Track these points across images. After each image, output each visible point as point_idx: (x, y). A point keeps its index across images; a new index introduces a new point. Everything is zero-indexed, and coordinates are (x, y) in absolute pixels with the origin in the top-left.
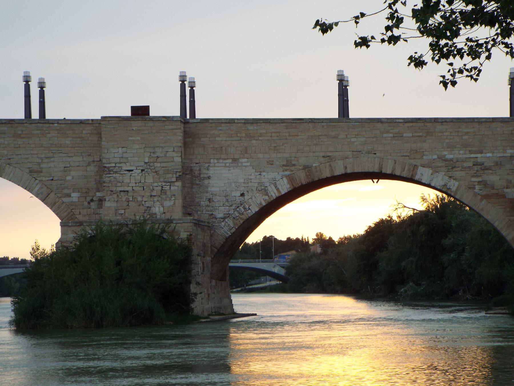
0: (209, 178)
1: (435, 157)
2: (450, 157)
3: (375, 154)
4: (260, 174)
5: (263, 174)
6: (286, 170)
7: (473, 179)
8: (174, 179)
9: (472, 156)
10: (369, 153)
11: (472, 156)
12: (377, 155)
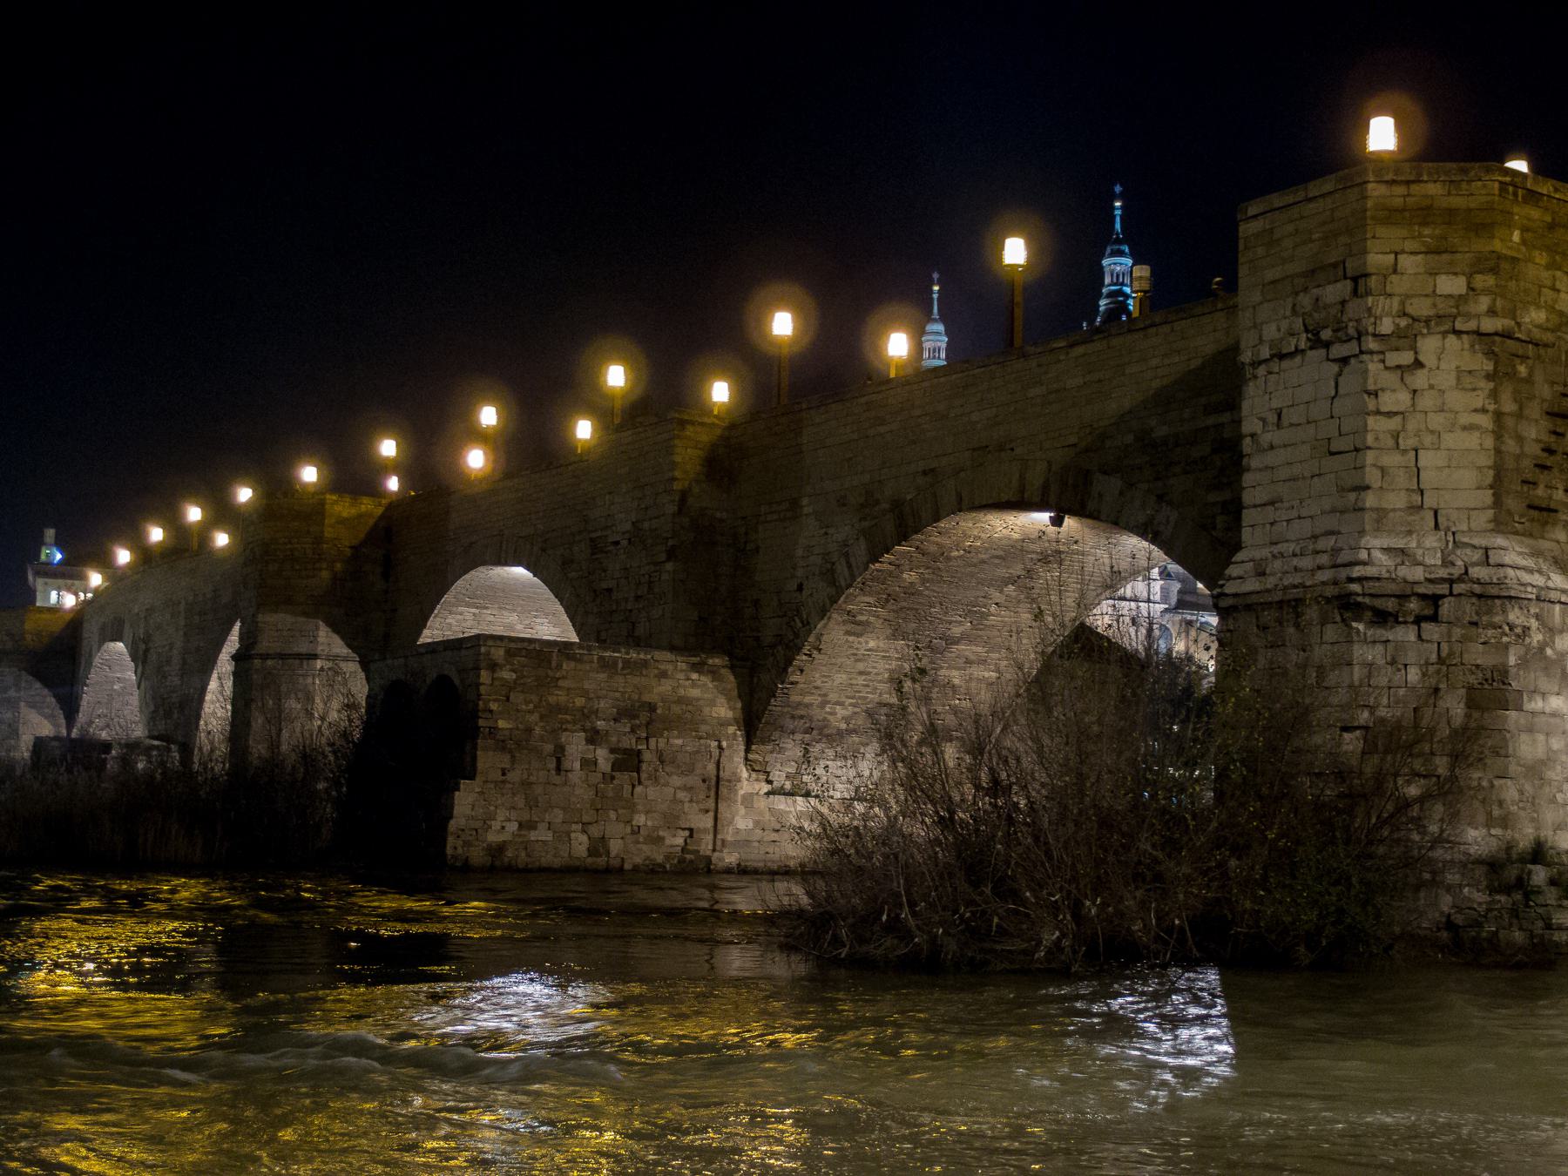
0: (757, 549)
1: (1130, 438)
2: (1161, 432)
3: (1012, 449)
4: (826, 534)
5: (831, 531)
6: (864, 519)
7: (1213, 497)
8: (663, 557)
9: (1211, 421)
10: (1001, 448)
11: (1211, 421)
12: (1018, 451)
